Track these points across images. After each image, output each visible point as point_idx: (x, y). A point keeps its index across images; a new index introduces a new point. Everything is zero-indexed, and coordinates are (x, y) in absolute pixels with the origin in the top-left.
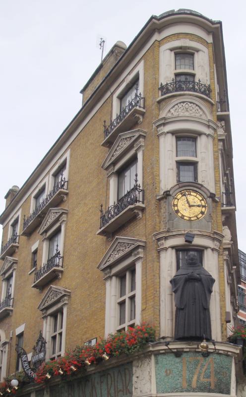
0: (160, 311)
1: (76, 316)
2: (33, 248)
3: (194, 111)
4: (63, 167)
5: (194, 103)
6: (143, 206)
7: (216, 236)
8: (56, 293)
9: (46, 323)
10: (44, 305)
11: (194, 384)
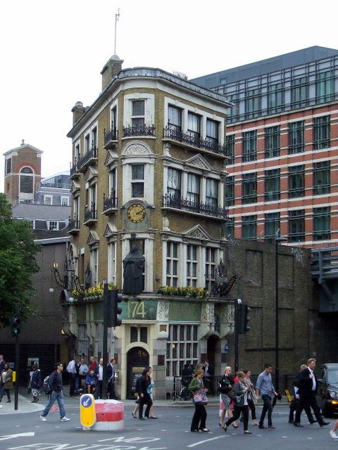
11: (133, 316)
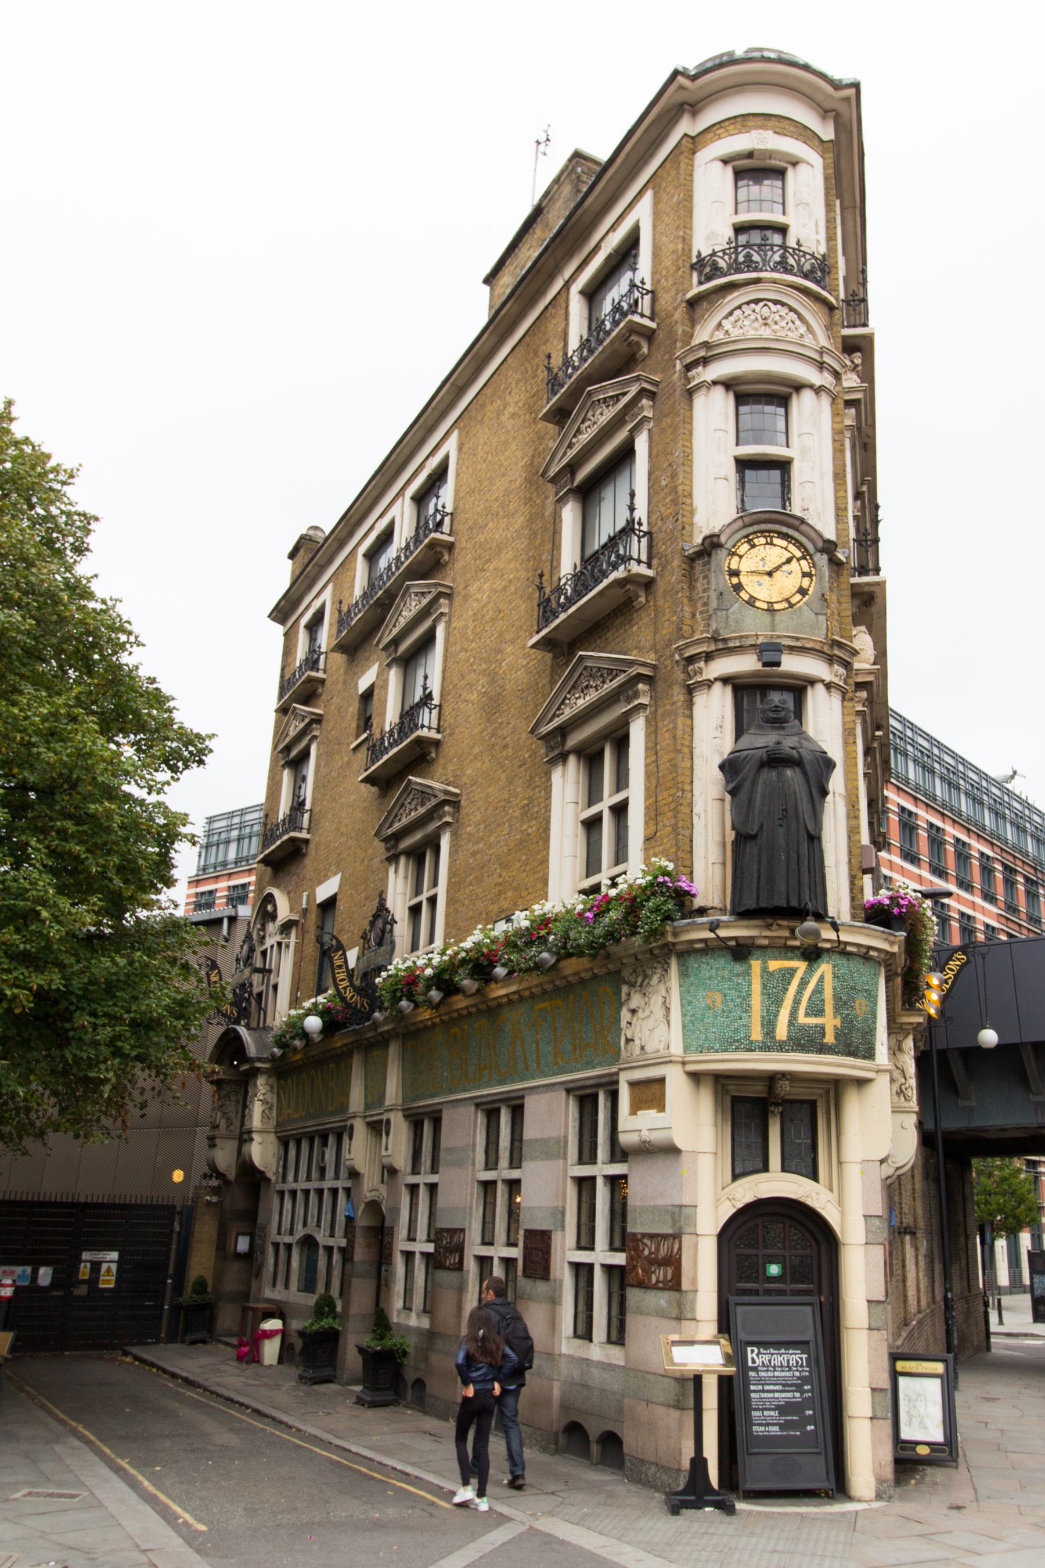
0: (691, 841)
1: (474, 854)
2: (363, 685)
3: (783, 324)
4: (439, 476)
5: (783, 304)
6: (650, 573)
7: (836, 652)
8: (425, 794)
9: (396, 871)
10: (391, 826)
11: (782, 1032)
